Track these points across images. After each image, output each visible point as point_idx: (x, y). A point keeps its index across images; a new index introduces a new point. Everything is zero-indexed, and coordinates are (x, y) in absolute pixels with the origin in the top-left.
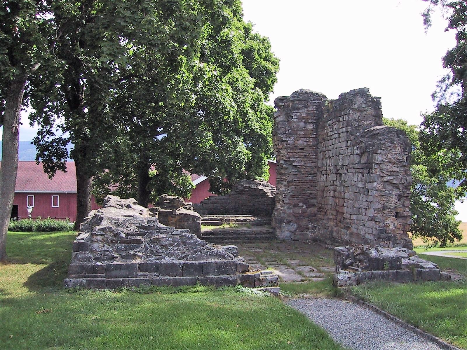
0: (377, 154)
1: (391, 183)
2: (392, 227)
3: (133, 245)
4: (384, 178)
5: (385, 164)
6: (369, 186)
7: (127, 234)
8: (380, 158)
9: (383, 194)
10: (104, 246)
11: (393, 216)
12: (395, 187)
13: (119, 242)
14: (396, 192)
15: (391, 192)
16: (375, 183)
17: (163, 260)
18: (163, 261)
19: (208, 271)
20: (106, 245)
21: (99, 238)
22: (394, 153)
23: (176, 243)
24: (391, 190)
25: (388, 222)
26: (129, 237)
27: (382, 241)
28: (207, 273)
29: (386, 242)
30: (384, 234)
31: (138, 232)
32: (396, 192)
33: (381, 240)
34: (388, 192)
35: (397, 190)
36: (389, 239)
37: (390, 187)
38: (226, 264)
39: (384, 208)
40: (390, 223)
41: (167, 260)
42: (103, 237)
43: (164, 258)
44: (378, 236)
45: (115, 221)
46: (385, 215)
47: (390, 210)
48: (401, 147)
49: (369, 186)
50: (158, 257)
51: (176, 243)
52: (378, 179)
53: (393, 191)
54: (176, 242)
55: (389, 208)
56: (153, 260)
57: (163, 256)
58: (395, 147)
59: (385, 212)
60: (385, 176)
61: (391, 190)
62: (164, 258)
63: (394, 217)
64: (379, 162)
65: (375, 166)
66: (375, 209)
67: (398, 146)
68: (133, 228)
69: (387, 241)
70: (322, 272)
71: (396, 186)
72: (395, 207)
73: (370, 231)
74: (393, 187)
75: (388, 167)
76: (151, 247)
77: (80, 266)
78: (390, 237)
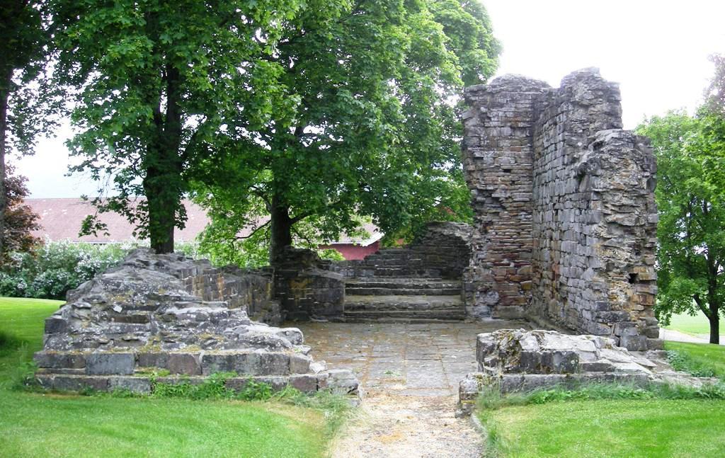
0: (597, 176)
1: (621, 226)
2: (622, 300)
3: (134, 324)
4: (608, 217)
5: (611, 193)
6: (587, 230)
7: (126, 308)
8: (602, 183)
9: (606, 243)
10: (89, 326)
11: (625, 280)
12: (627, 231)
13: (113, 319)
14: (630, 240)
15: (620, 240)
16: (595, 226)
17: (175, 349)
18: (175, 351)
19: (242, 369)
20: (93, 324)
21: (83, 313)
22: (624, 173)
23: (202, 323)
24: (620, 237)
25: (615, 290)
26: (129, 312)
27: (603, 323)
28: (239, 372)
29: (609, 324)
30: (606, 311)
31: (145, 305)
32: (630, 240)
33: (600, 320)
34: (615, 240)
35: (632, 237)
36: (614, 319)
37: (618, 232)
38: (272, 358)
39: (610, 266)
40: (619, 293)
41: (183, 349)
42: (88, 312)
43: (177, 346)
44: (596, 314)
45: (113, 287)
46: (610, 278)
47: (618, 270)
48: (637, 164)
49: (587, 230)
50: (168, 344)
51: (202, 323)
52: (600, 218)
53: (624, 238)
54: (202, 321)
55: (618, 268)
56: (162, 348)
57: (177, 342)
58: (626, 165)
59: (611, 274)
60: (610, 212)
61: (620, 237)
62: (177, 346)
63: (626, 283)
64: (600, 190)
65: (595, 196)
66: (595, 269)
67: (633, 162)
68: (140, 299)
69: (610, 322)
70: (488, 371)
71: (629, 230)
72: (629, 266)
73: (588, 305)
74: (625, 231)
75: (616, 198)
76: (162, 328)
77: (48, 355)
78: (617, 315)
